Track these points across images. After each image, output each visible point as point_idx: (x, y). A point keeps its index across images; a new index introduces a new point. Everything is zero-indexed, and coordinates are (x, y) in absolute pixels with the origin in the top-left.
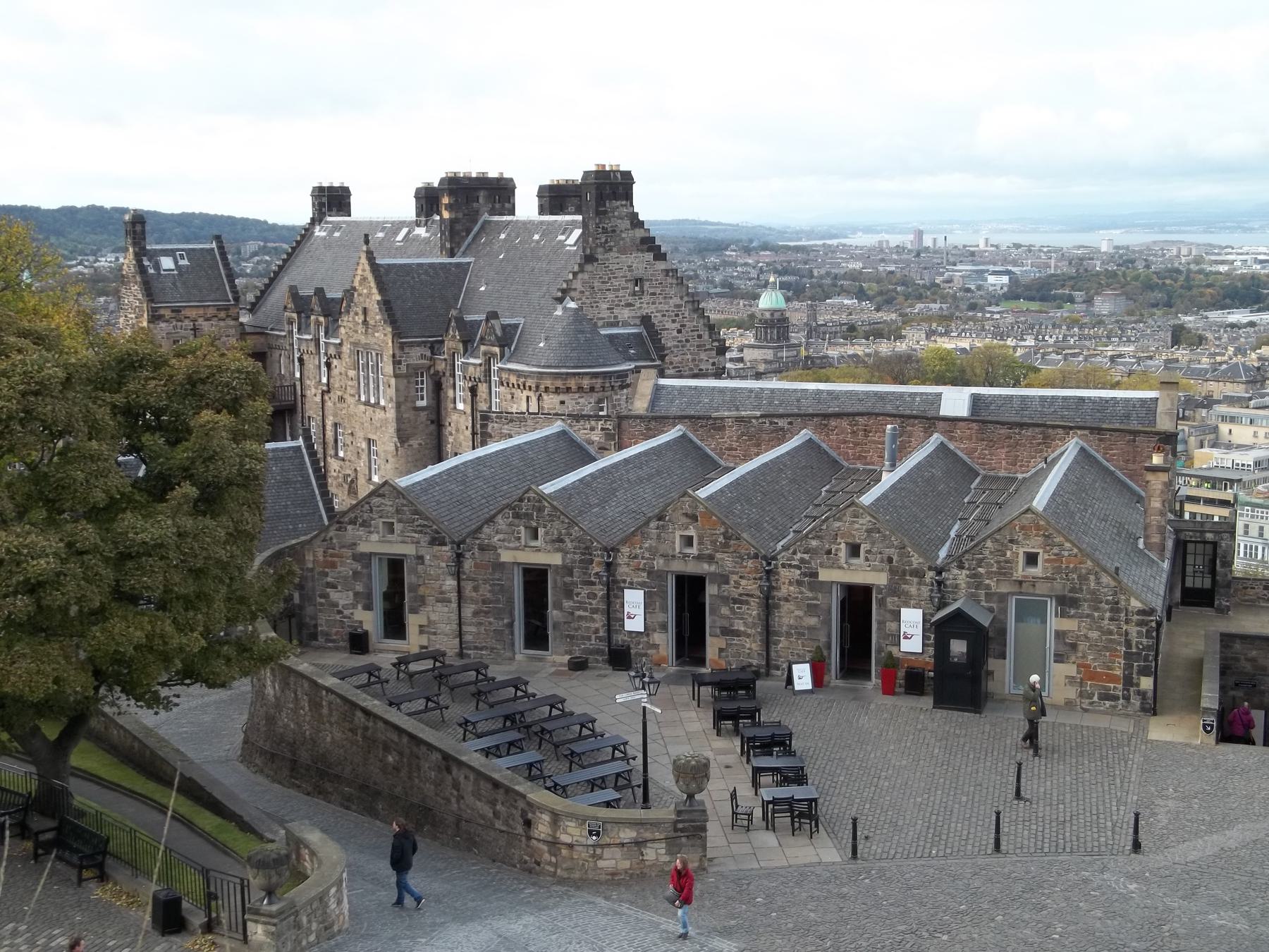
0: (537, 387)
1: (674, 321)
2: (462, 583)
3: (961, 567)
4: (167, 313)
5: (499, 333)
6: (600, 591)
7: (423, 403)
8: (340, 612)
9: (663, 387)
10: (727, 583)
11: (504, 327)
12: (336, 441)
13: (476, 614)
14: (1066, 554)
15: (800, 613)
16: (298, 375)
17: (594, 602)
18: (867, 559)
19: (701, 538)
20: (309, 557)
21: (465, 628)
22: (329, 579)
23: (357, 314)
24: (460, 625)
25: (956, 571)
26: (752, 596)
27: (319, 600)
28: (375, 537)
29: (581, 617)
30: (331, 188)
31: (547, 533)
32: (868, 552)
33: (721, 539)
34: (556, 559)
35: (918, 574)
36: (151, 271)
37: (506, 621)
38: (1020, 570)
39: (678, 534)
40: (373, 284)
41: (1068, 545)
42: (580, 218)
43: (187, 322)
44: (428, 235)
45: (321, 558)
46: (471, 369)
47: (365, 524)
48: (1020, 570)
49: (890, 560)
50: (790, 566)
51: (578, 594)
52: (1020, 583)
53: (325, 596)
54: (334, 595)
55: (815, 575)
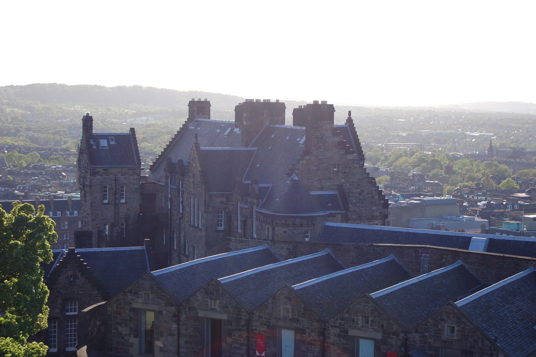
0: (272, 222)
1: (357, 188)
2: (180, 327)
3: (417, 332)
4: (101, 170)
5: (257, 191)
6: (245, 334)
7: (222, 228)
8: (123, 338)
9: (328, 227)
10: (305, 333)
11: (261, 189)
12: (185, 246)
13: (186, 342)
14: (467, 328)
15: (339, 352)
16: (169, 207)
17: (241, 340)
18: (372, 325)
19: (292, 309)
20: (109, 309)
21: (181, 350)
22: (119, 320)
23: (190, 177)
24: (179, 347)
25: (415, 334)
26: (316, 341)
27: (113, 331)
28: (140, 300)
29: (235, 348)
30: (199, 102)
31: (220, 303)
32: (372, 321)
33: (302, 310)
34: (224, 317)
35: (396, 334)
36: (95, 147)
37: (200, 347)
38: (446, 334)
39: (282, 307)
40: (197, 162)
41: (468, 323)
42: (304, 128)
43: (111, 176)
44: (239, 132)
45: (115, 310)
46: (244, 210)
47: (136, 293)
48: (446, 334)
49: (383, 326)
50: (335, 326)
51: (234, 335)
52: (445, 342)
53: (116, 329)
54: (120, 329)
55: (347, 332)
